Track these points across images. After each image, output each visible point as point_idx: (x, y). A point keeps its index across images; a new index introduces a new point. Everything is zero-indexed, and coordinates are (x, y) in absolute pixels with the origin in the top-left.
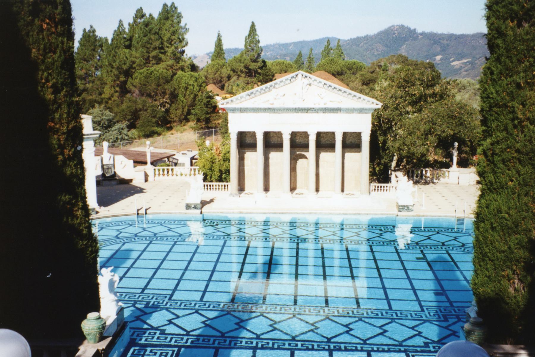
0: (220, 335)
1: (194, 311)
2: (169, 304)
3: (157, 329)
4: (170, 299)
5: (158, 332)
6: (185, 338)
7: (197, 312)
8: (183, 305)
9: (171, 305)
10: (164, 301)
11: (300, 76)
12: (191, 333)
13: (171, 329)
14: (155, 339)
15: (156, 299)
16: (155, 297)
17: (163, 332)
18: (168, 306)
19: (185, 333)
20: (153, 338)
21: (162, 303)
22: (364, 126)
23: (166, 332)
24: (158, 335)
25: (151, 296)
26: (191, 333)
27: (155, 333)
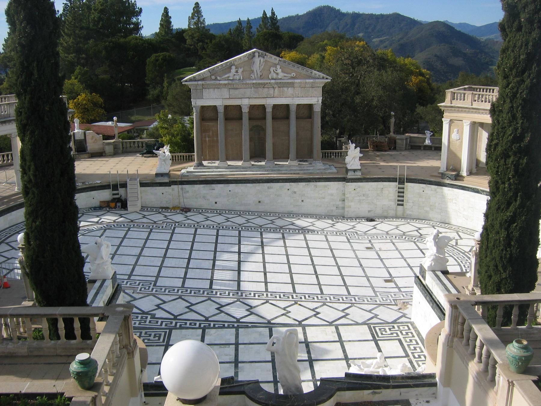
0: (204, 319)
1: (178, 297)
2: (155, 290)
3: (147, 313)
4: (155, 285)
5: (149, 317)
6: (174, 322)
7: (180, 297)
8: (167, 290)
9: (156, 291)
10: (149, 287)
11: (257, 54)
12: (178, 317)
13: (160, 314)
14: (147, 323)
15: (143, 285)
16: (141, 284)
17: (153, 316)
18: (154, 292)
19: (173, 317)
20: (145, 322)
21: (149, 289)
22: (315, 99)
23: (156, 316)
24: (149, 319)
25: (138, 282)
26: (178, 317)
27: (147, 318)
